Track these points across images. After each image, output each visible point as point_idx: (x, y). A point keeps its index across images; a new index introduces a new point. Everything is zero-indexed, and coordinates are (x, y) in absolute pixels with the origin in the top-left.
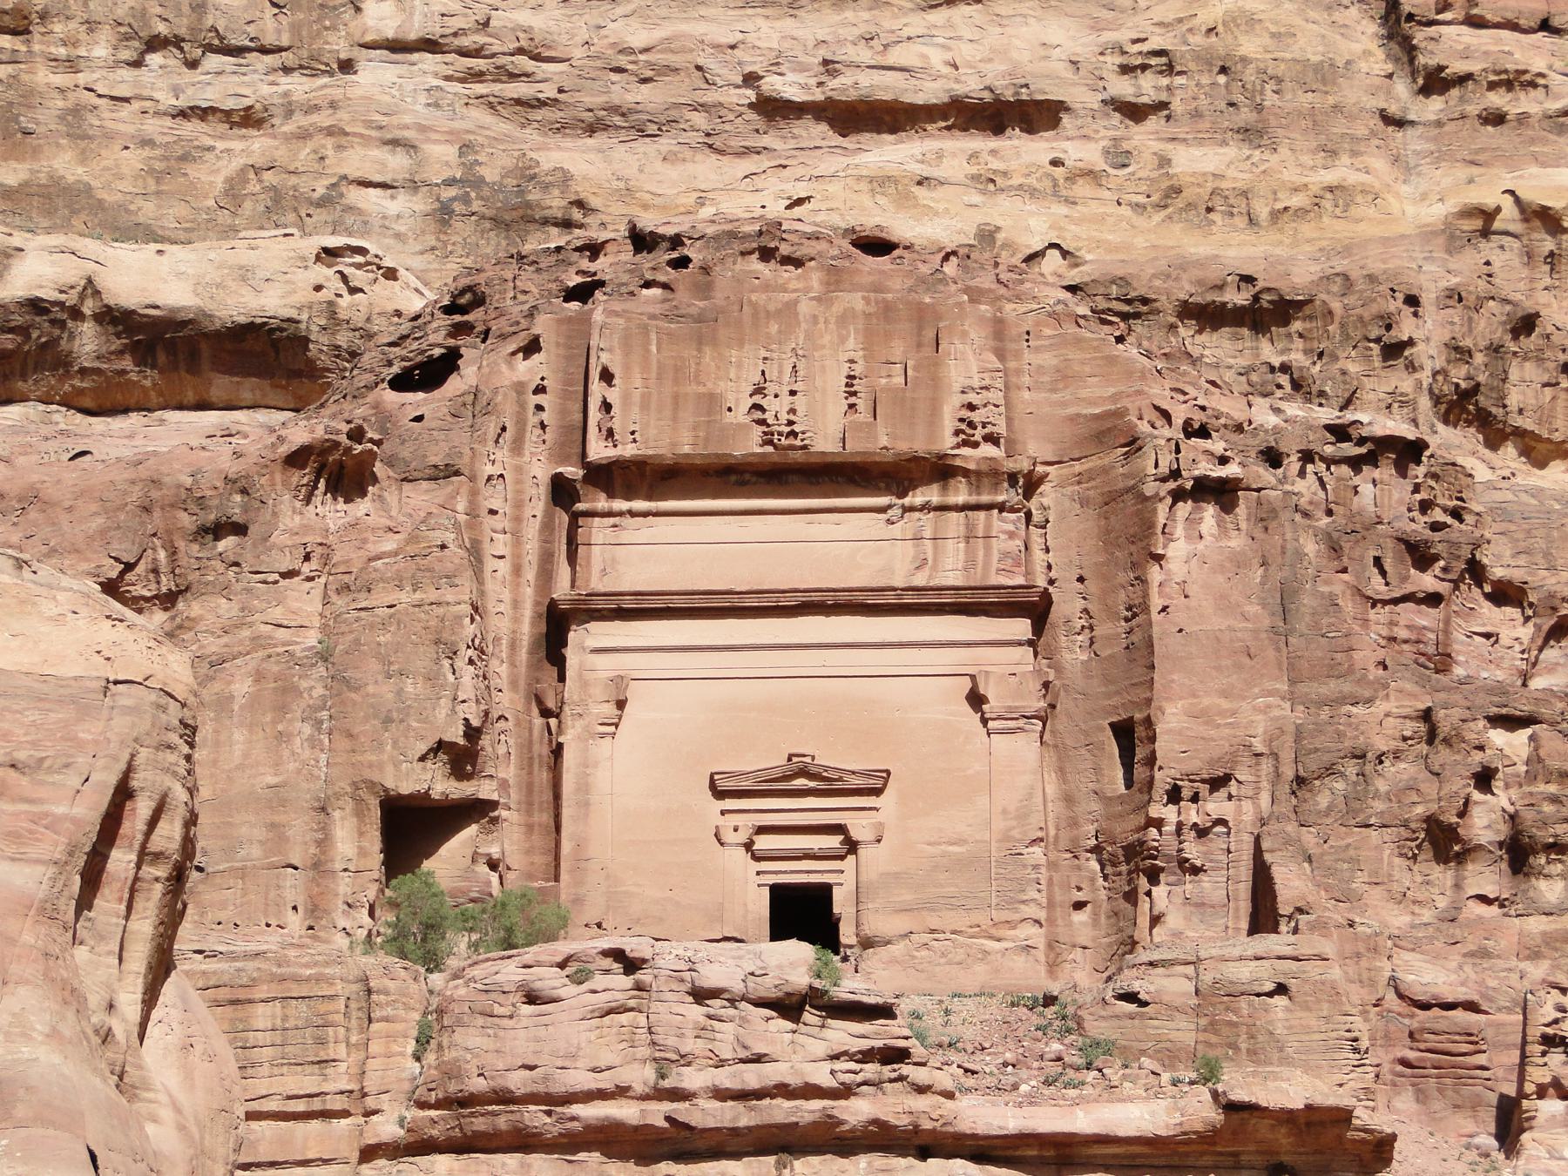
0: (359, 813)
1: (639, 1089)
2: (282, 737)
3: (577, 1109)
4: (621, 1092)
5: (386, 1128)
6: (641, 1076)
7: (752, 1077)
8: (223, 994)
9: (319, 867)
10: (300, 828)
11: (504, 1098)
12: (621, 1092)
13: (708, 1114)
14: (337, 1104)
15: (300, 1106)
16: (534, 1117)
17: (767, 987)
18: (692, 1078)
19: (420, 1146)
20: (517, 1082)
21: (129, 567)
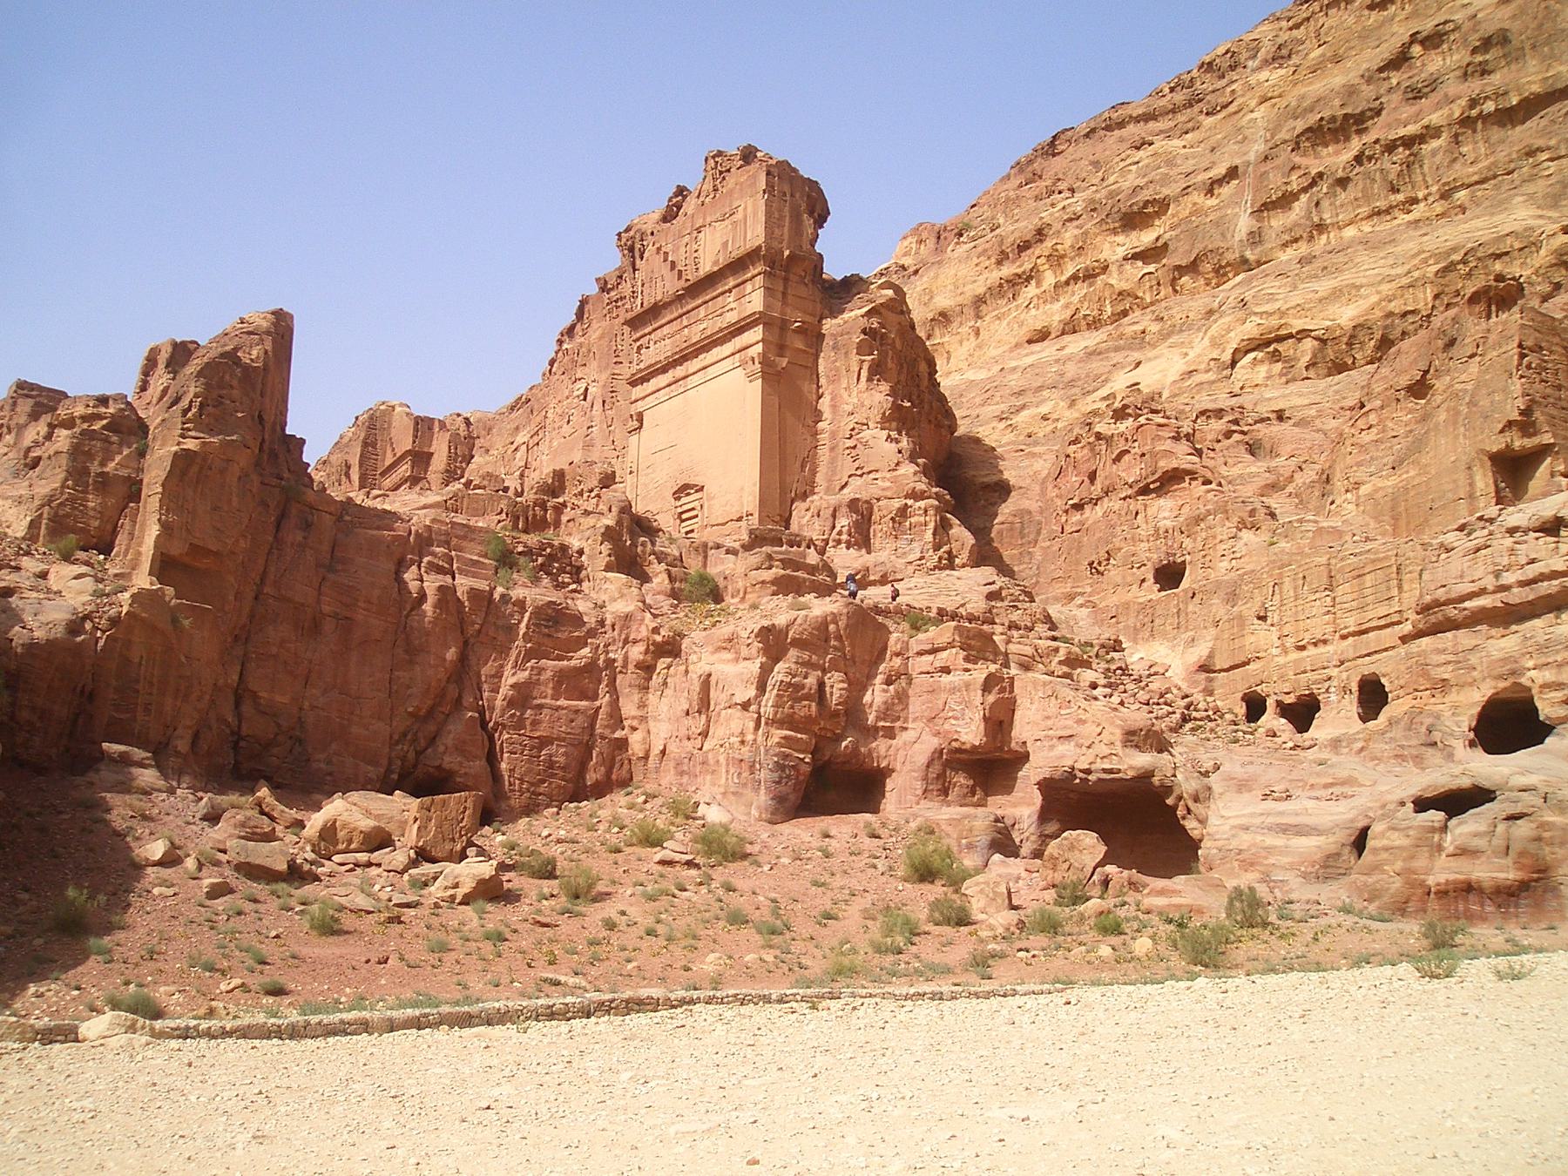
0: (1482, 466)
1: (1491, 588)
2: (1456, 437)
3: (1467, 604)
4: (1483, 592)
5: (1407, 628)
6: (1489, 583)
7: (1532, 571)
8: (1355, 573)
9: (1471, 496)
10: (1462, 477)
11: (1438, 604)
12: (1483, 592)
13: (1517, 596)
14: (1396, 618)
15: (1382, 622)
16: (1451, 611)
17: (1535, 523)
18: (1509, 578)
19: (1419, 634)
20: (1441, 594)
21: (1426, 372)
